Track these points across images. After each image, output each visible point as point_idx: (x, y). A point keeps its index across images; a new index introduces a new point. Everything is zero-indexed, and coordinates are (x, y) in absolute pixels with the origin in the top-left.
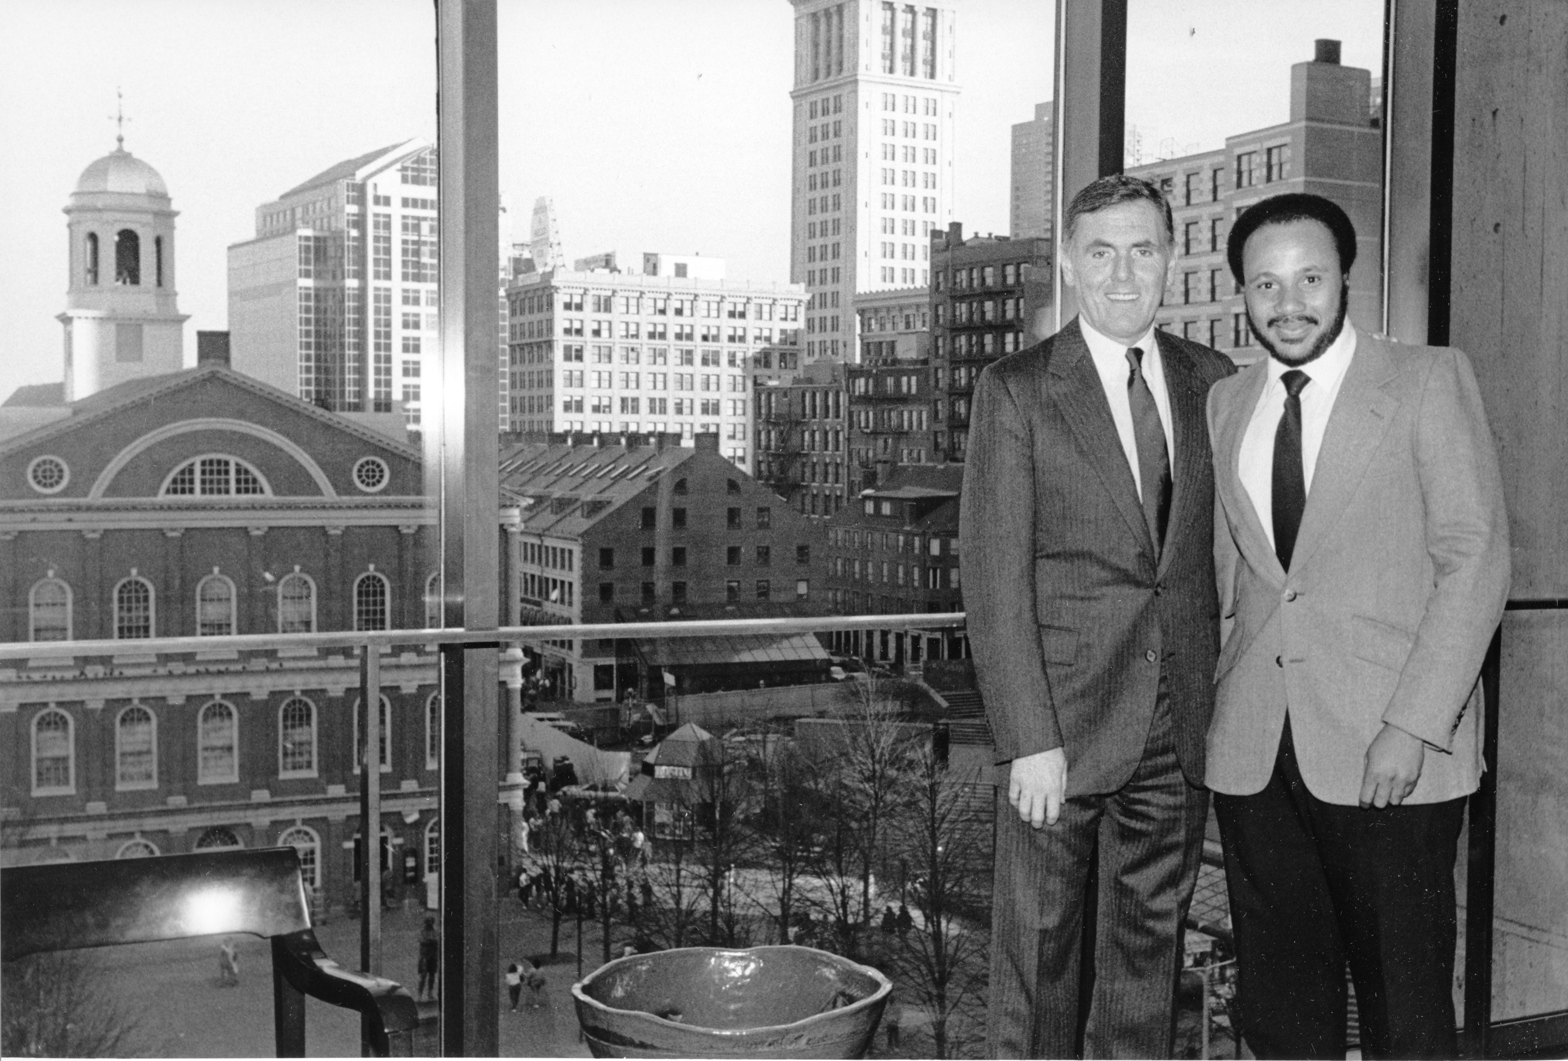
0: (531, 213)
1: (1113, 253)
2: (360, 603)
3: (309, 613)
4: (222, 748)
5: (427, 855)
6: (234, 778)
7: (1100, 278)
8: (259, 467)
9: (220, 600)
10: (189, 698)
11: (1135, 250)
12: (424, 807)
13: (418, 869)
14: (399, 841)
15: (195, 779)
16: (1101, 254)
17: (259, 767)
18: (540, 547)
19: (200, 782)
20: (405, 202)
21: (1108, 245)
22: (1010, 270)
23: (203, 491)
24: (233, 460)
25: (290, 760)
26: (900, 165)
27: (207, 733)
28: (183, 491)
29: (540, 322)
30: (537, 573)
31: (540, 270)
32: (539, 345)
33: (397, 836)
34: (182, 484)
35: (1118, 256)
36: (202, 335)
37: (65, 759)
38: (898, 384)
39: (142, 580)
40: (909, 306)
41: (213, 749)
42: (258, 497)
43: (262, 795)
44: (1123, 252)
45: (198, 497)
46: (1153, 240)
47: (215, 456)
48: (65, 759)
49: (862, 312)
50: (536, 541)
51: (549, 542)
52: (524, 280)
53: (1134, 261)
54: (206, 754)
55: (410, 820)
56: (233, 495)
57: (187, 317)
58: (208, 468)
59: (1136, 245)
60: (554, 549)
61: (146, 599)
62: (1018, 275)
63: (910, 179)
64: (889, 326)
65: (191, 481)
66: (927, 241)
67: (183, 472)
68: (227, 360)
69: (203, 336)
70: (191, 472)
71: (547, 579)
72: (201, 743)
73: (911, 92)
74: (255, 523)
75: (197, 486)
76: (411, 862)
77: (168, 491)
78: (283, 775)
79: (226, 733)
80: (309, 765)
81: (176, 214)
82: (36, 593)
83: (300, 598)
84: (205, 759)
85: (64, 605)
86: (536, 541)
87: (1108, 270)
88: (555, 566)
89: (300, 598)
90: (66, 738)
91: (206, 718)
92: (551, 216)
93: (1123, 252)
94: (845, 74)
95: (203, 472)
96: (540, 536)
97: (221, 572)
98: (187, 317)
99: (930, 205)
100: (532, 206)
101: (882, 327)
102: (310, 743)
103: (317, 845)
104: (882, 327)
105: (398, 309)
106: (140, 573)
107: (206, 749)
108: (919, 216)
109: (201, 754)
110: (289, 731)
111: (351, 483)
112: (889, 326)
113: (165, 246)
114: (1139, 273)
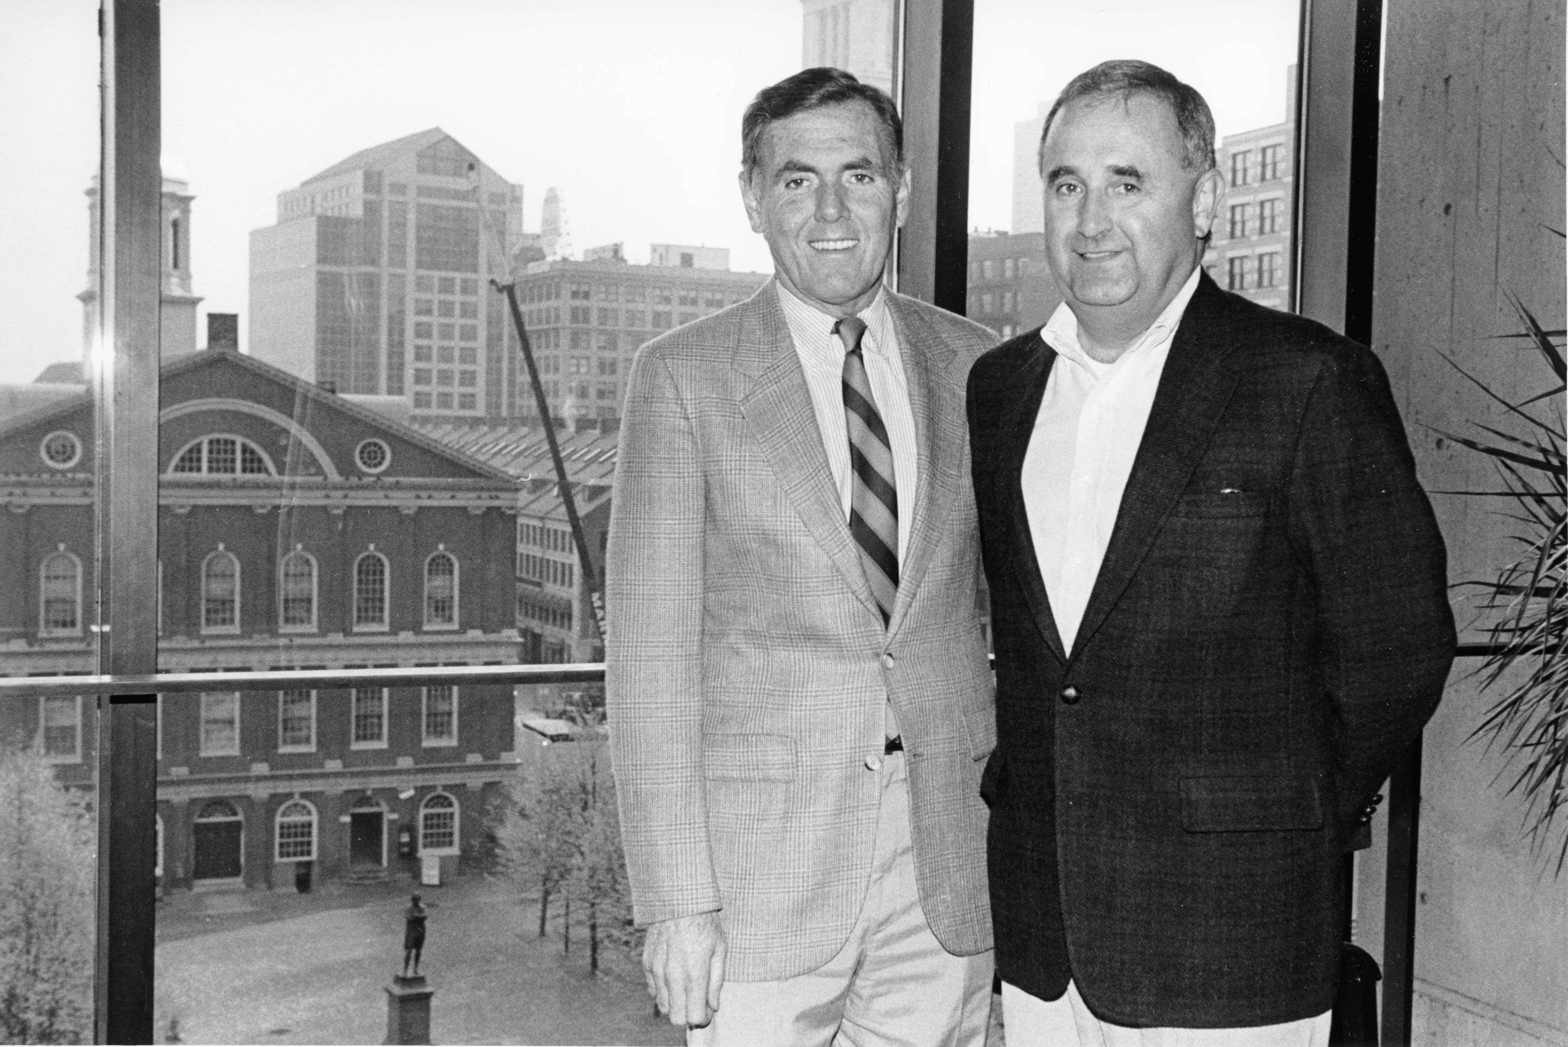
0: (541, 203)
2: (360, 581)
3: (311, 590)
5: (421, 831)
6: (235, 751)
7: (799, 218)
8: (265, 448)
9: (224, 576)
11: (848, 173)
12: (419, 784)
13: (412, 845)
14: (394, 816)
15: (197, 748)
17: (259, 740)
18: (542, 529)
19: (203, 754)
20: (422, 191)
22: (1009, 263)
24: (239, 440)
25: (289, 734)
28: (191, 470)
29: (548, 310)
30: (539, 555)
31: (550, 259)
32: (547, 332)
33: (393, 811)
34: (190, 462)
37: (73, 728)
41: (215, 721)
42: (262, 477)
43: (261, 768)
44: (830, 178)
45: (204, 475)
46: (875, 160)
47: (223, 436)
48: (73, 728)
50: (538, 523)
51: (550, 525)
52: (533, 268)
53: (846, 190)
54: (210, 727)
55: (404, 796)
56: (239, 474)
57: (200, 300)
58: (215, 446)
59: (850, 167)
60: (556, 532)
62: (1016, 269)
65: (199, 460)
69: (212, 317)
70: (199, 451)
71: (548, 561)
72: (203, 714)
74: (260, 502)
75: (205, 465)
76: (405, 838)
77: (177, 469)
78: (283, 750)
79: (227, 706)
80: (308, 740)
81: (190, 199)
82: (48, 566)
83: (302, 575)
84: (207, 731)
85: (74, 577)
86: (538, 523)
88: (556, 548)
89: (302, 575)
90: (74, 708)
92: (562, 205)
93: (830, 178)
96: (542, 519)
97: (227, 548)
98: (200, 300)
100: (542, 196)
102: (308, 718)
103: (314, 818)
105: (411, 295)
107: (208, 722)
109: (203, 727)
110: (290, 706)
111: (353, 464)
113: (181, 229)
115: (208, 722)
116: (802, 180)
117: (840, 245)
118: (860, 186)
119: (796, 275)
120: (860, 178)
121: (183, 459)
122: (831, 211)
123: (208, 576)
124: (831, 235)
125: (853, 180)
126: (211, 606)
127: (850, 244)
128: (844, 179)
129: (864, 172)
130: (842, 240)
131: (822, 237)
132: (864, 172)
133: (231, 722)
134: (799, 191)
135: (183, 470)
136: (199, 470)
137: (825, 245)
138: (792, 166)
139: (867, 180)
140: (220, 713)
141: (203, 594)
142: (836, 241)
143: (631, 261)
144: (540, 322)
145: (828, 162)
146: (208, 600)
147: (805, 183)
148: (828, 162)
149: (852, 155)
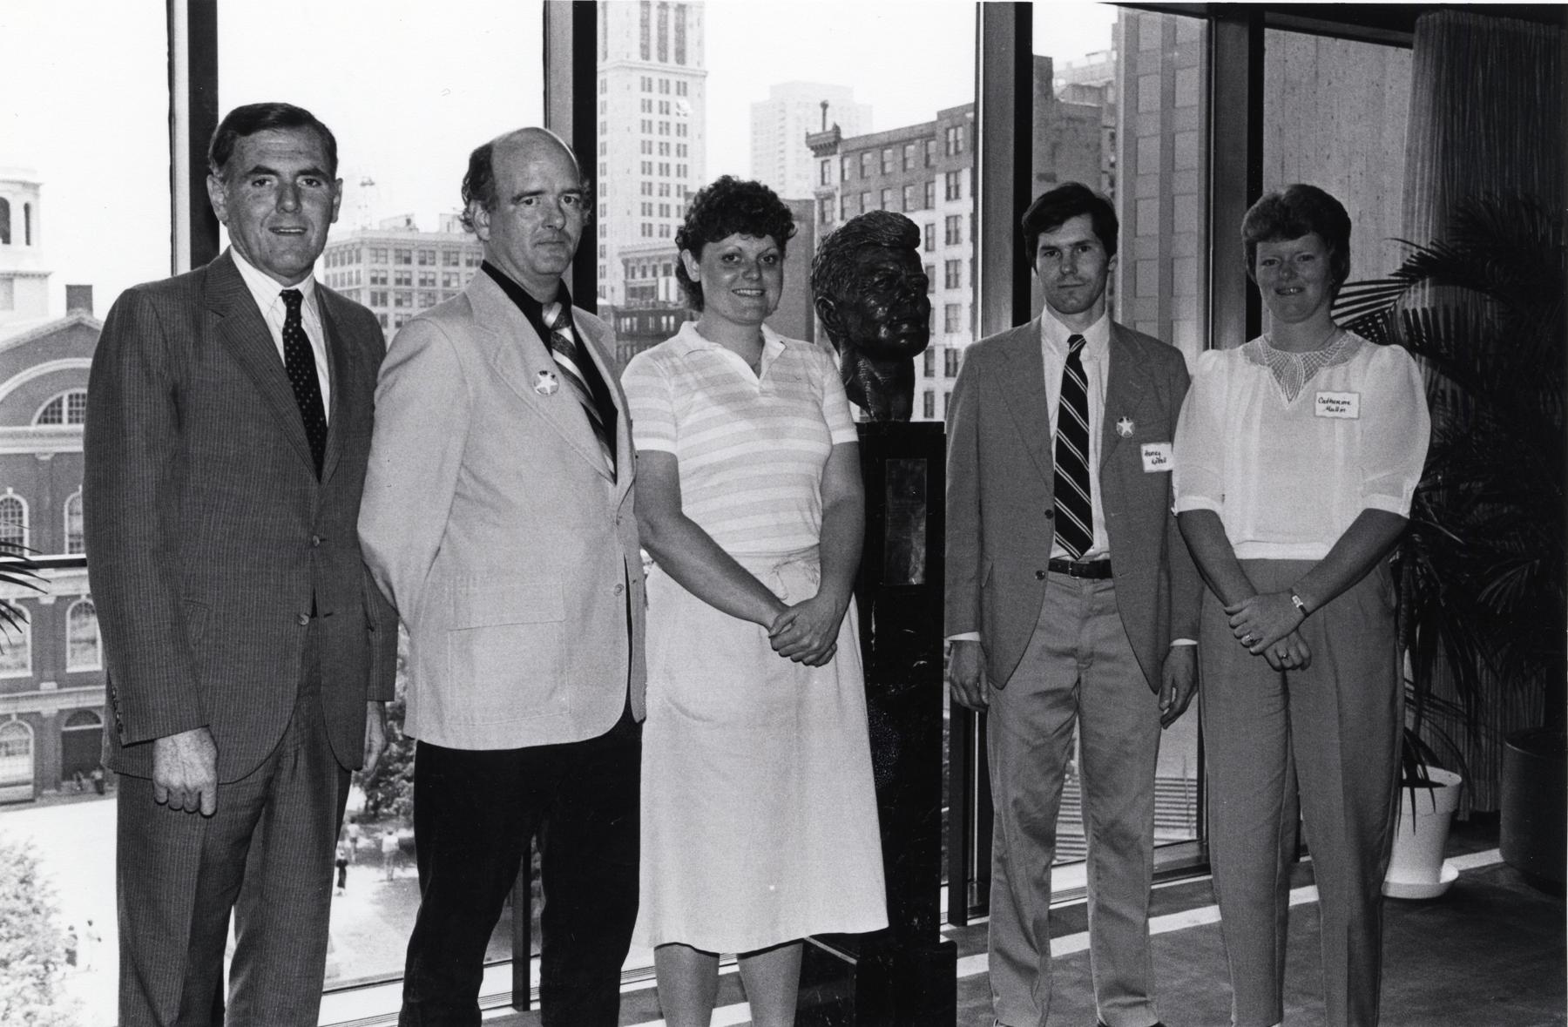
1: (275, 181)
4: (87, 641)
10: (59, 598)
23: (70, 421)
26: (656, 138)
27: (74, 628)
28: (53, 421)
35: (282, 183)
36: (69, 288)
38: (658, 323)
39: (17, 497)
40: (666, 257)
41: (80, 641)
44: (288, 179)
49: (626, 262)
59: (302, 173)
61: (21, 514)
63: (665, 148)
64: (649, 274)
66: (681, 201)
67: (52, 405)
68: (90, 309)
72: (69, 635)
73: (664, 77)
77: (39, 422)
87: (272, 200)
91: (73, 615)
94: (609, 61)
95: (71, 405)
99: (682, 171)
101: (644, 275)
104: (644, 275)
106: (15, 492)
108: (673, 180)
109: (69, 646)
112: (649, 274)
114: (306, 205)
115: (73, 642)
121: (45, 412)
122: (290, 204)
123: (71, 514)
126: (74, 541)
133: (94, 642)
135: (46, 421)
136: (60, 421)
138: (259, 170)
140: (83, 634)
141: (66, 530)
143: (422, 230)
144: (343, 284)
145: (286, 168)
146: (71, 536)
148: (286, 168)
149: (306, 164)
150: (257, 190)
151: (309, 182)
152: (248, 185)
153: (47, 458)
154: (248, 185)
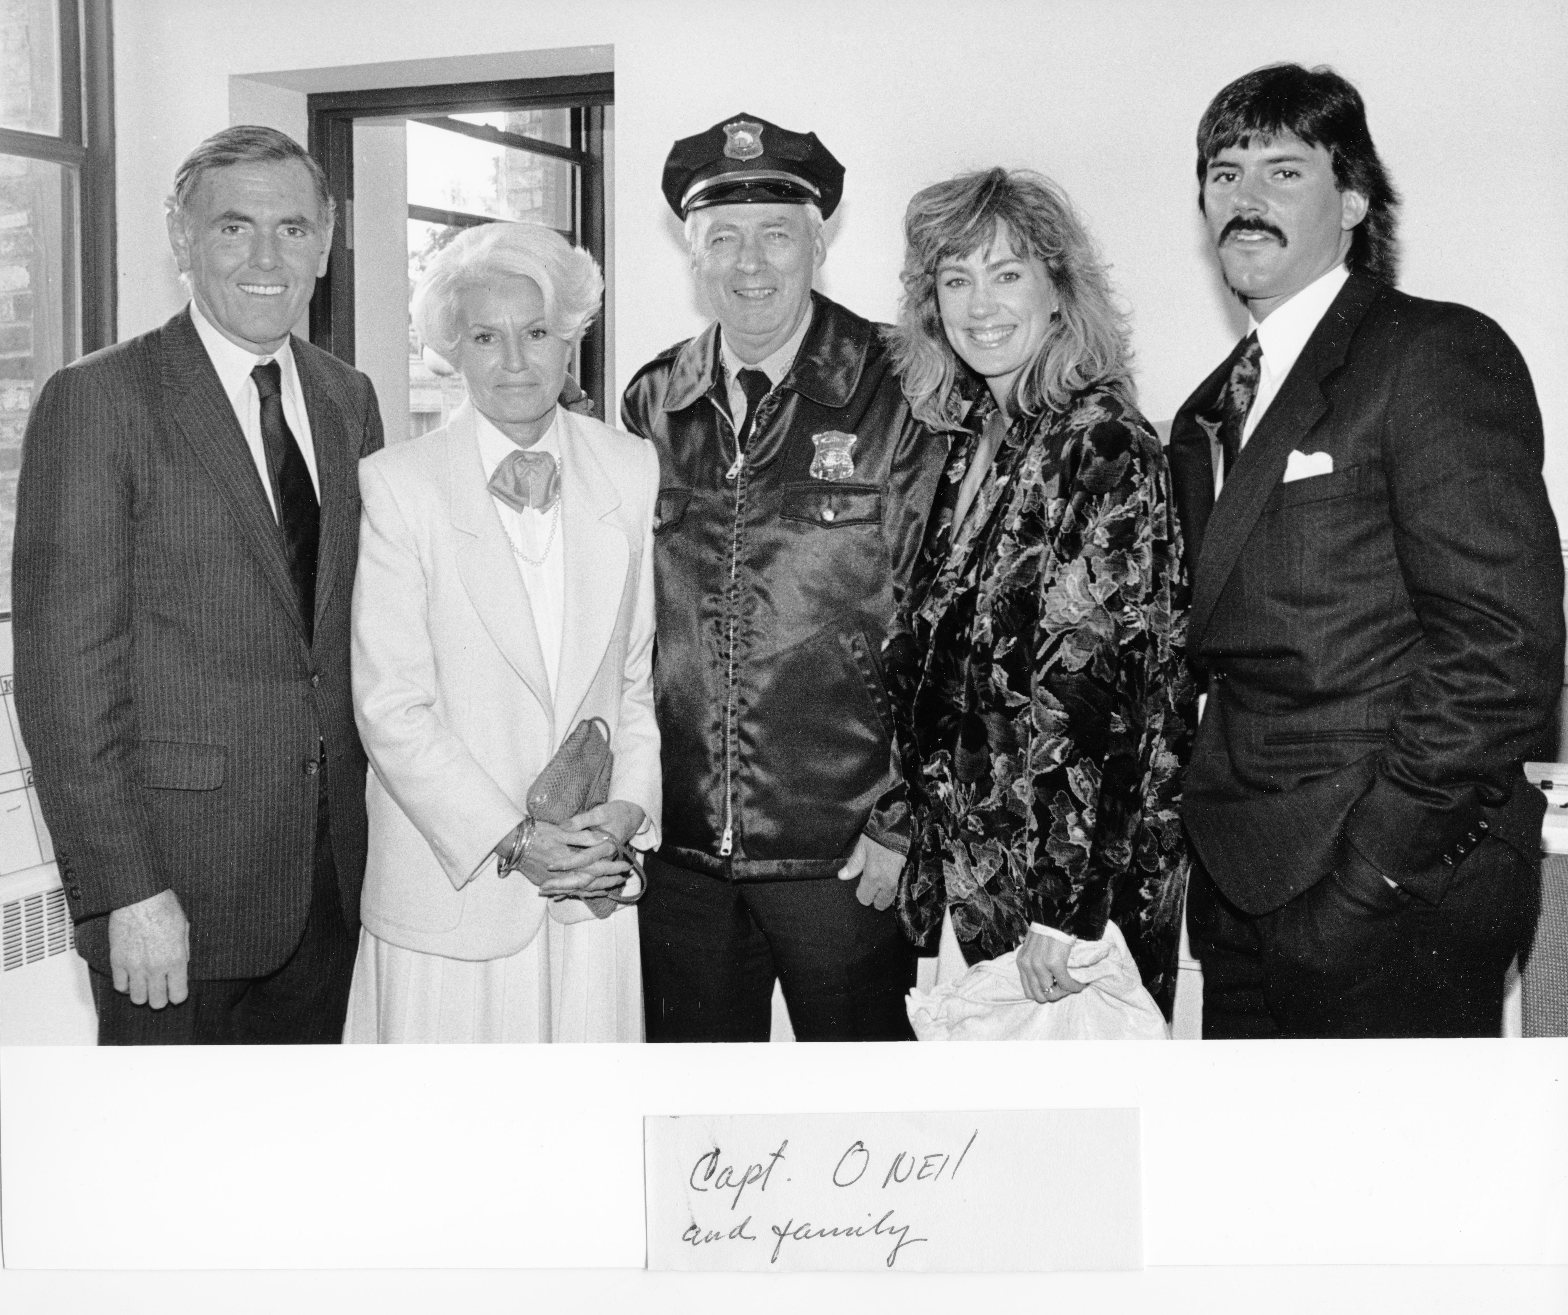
16: (234, 229)
21: (246, 219)
44: (266, 230)
53: (279, 240)
59: (284, 222)
116: (237, 227)
117: (270, 291)
118: (292, 239)
119: (222, 312)
120: (292, 232)
124: (262, 282)
125: (286, 233)
127: (278, 290)
128: (278, 231)
129: (297, 227)
130: (272, 285)
131: (255, 281)
132: (297, 227)
134: (234, 237)
137: (256, 289)
138: (232, 215)
139: (299, 233)
142: (266, 286)
147: (241, 231)
150: (229, 237)
151: (292, 232)
152: (217, 232)
153: (792, 380)
154: (217, 232)
